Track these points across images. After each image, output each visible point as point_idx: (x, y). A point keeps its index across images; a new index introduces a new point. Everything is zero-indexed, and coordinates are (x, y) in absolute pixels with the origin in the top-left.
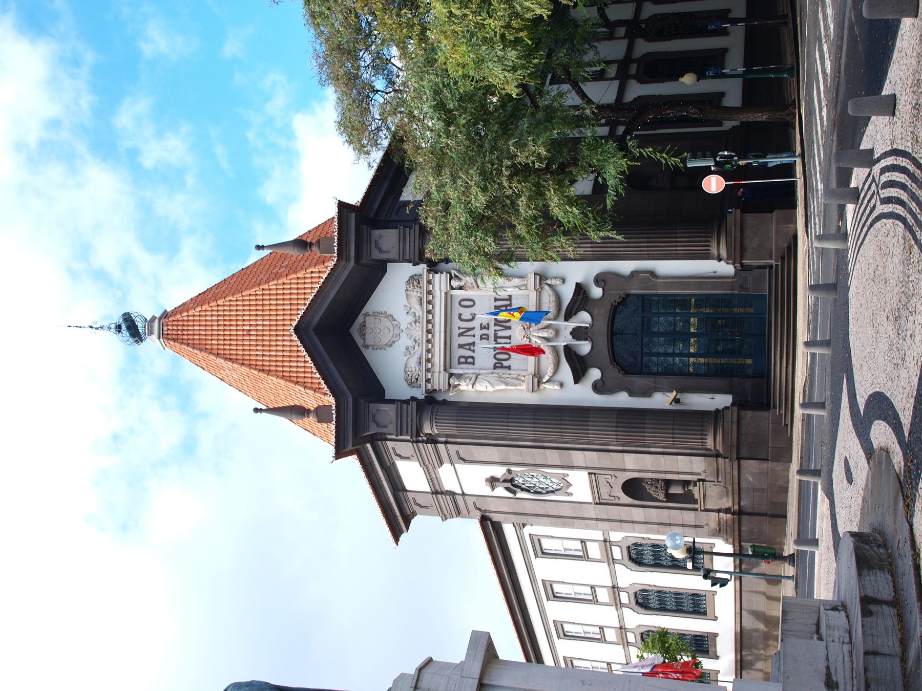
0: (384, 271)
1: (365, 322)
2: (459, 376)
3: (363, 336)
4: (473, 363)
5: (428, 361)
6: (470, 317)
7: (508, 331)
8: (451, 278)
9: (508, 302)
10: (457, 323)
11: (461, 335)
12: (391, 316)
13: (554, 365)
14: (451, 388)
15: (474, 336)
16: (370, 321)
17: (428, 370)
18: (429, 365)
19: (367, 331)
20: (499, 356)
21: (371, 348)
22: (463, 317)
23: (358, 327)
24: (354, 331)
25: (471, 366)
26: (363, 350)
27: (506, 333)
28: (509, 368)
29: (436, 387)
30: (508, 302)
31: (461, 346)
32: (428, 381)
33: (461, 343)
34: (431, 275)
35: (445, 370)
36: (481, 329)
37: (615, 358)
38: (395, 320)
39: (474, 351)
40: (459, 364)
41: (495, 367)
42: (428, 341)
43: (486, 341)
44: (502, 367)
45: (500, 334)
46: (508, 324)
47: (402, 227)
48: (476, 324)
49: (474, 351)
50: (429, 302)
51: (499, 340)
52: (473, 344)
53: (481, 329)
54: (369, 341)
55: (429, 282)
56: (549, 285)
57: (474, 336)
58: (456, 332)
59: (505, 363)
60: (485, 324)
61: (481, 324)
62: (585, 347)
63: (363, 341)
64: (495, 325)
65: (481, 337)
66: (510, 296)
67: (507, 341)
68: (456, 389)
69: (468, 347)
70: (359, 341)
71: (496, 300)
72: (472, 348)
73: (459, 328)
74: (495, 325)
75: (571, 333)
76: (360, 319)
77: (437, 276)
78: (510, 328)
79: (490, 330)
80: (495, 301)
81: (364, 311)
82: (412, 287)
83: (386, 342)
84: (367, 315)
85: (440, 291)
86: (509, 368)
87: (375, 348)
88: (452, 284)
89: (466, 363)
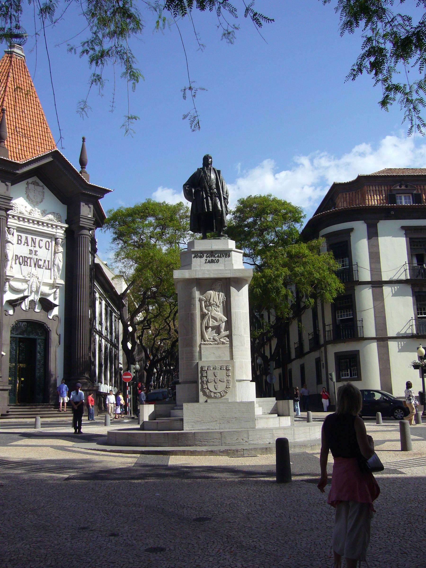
0: (64, 203)
1: (40, 186)
2: (13, 234)
3: (34, 183)
4: (18, 243)
5: (24, 219)
6: (41, 246)
7: (34, 266)
8: (62, 239)
9: (47, 268)
10: (38, 238)
11: (32, 239)
12: (42, 201)
13: (18, 289)
14: (7, 229)
15: (32, 246)
16: (39, 189)
17: (19, 218)
18: (21, 219)
19: (36, 186)
20: (21, 258)
21: (27, 186)
22: (41, 241)
23: (37, 181)
24: (35, 179)
25: (17, 242)
26: (25, 182)
27: (33, 265)
28: (16, 264)
29: (9, 220)
30: (47, 268)
31: (27, 238)
32: (13, 216)
33: (28, 238)
34: (65, 229)
35: (18, 227)
36: (35, 251)
37: (19, 322)
38: (40, 203)
39: (24, 245)
40: (18, 235)
41: (16, 256)
42: (29, 220)
43: (29, 253)
44: (16, 260)
45: (32, 261)
46: (37, 266)
47: (94, 220)
48: (37, 248)
49: (24, 245)
50: (52, 225)
51: (29, 260)
52: (28, 245)
53: (35, 251)
54: (31, 186)
55: (61, 227)
56: (56, 291)
57: (32, 246)
58: (34, 237)
59: (17, 261)
60: (37, 253)
61: (37, 251)
62: (25, 306)
63: (30, 182)
64: (37, 259)
65: (32, 250)
66: (51, 269)
67: (29, 264)
68: (7, 231)
69: (26, 242)
70: (30, 180)
71: (48, 261)
72: (26, 244)
73: (35, 239)
74: (37, 259)
75: (33, 300)
76: (41, 183)
77: (63, 232)
78: (35, 267)
79: (34, 255)
80: (48, 261)
81: (45, 187)
82: (58, 217)
83: (30, 195)
84: (43, 189)
85: (56, 233)
86: (16, 264)
87: (27, 188)
88: (59, 239)
89: (18, 240)
